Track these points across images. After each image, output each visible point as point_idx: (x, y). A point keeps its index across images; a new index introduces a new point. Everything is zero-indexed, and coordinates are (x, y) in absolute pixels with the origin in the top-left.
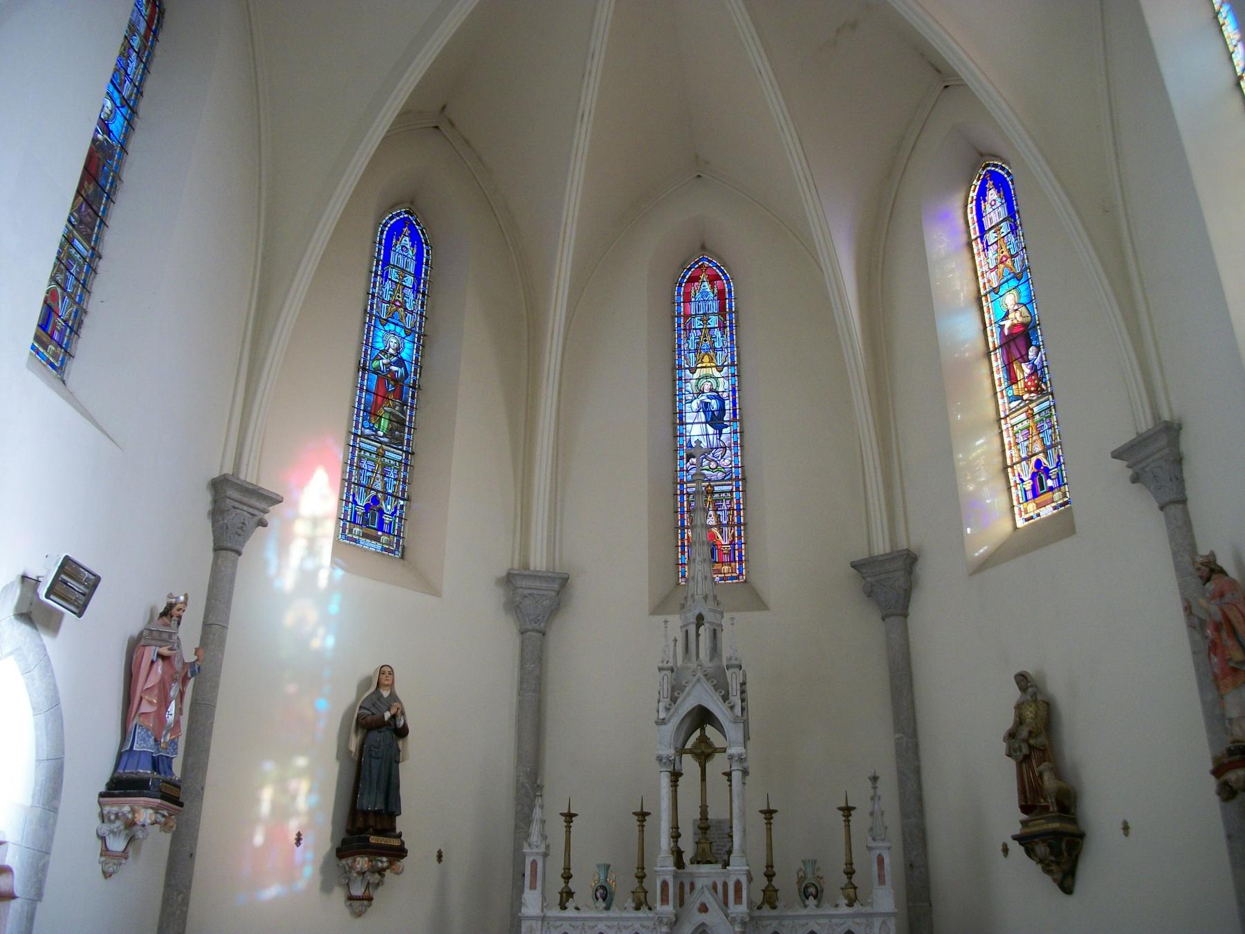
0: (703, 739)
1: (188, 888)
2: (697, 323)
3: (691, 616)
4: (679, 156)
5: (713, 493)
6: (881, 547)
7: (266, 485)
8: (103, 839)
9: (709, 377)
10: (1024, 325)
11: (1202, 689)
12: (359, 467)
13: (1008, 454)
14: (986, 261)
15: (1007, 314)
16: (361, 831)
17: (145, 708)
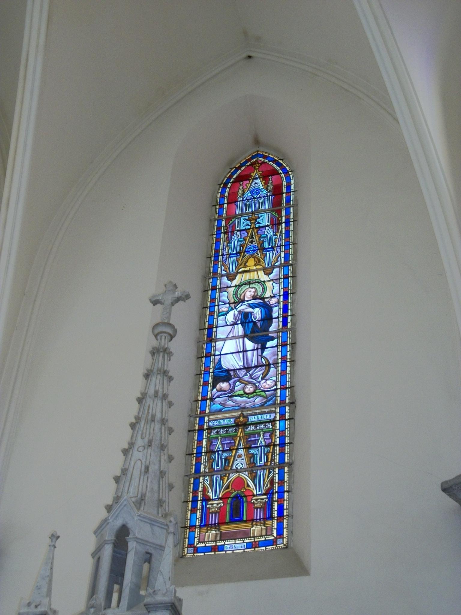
5: (246, 425)
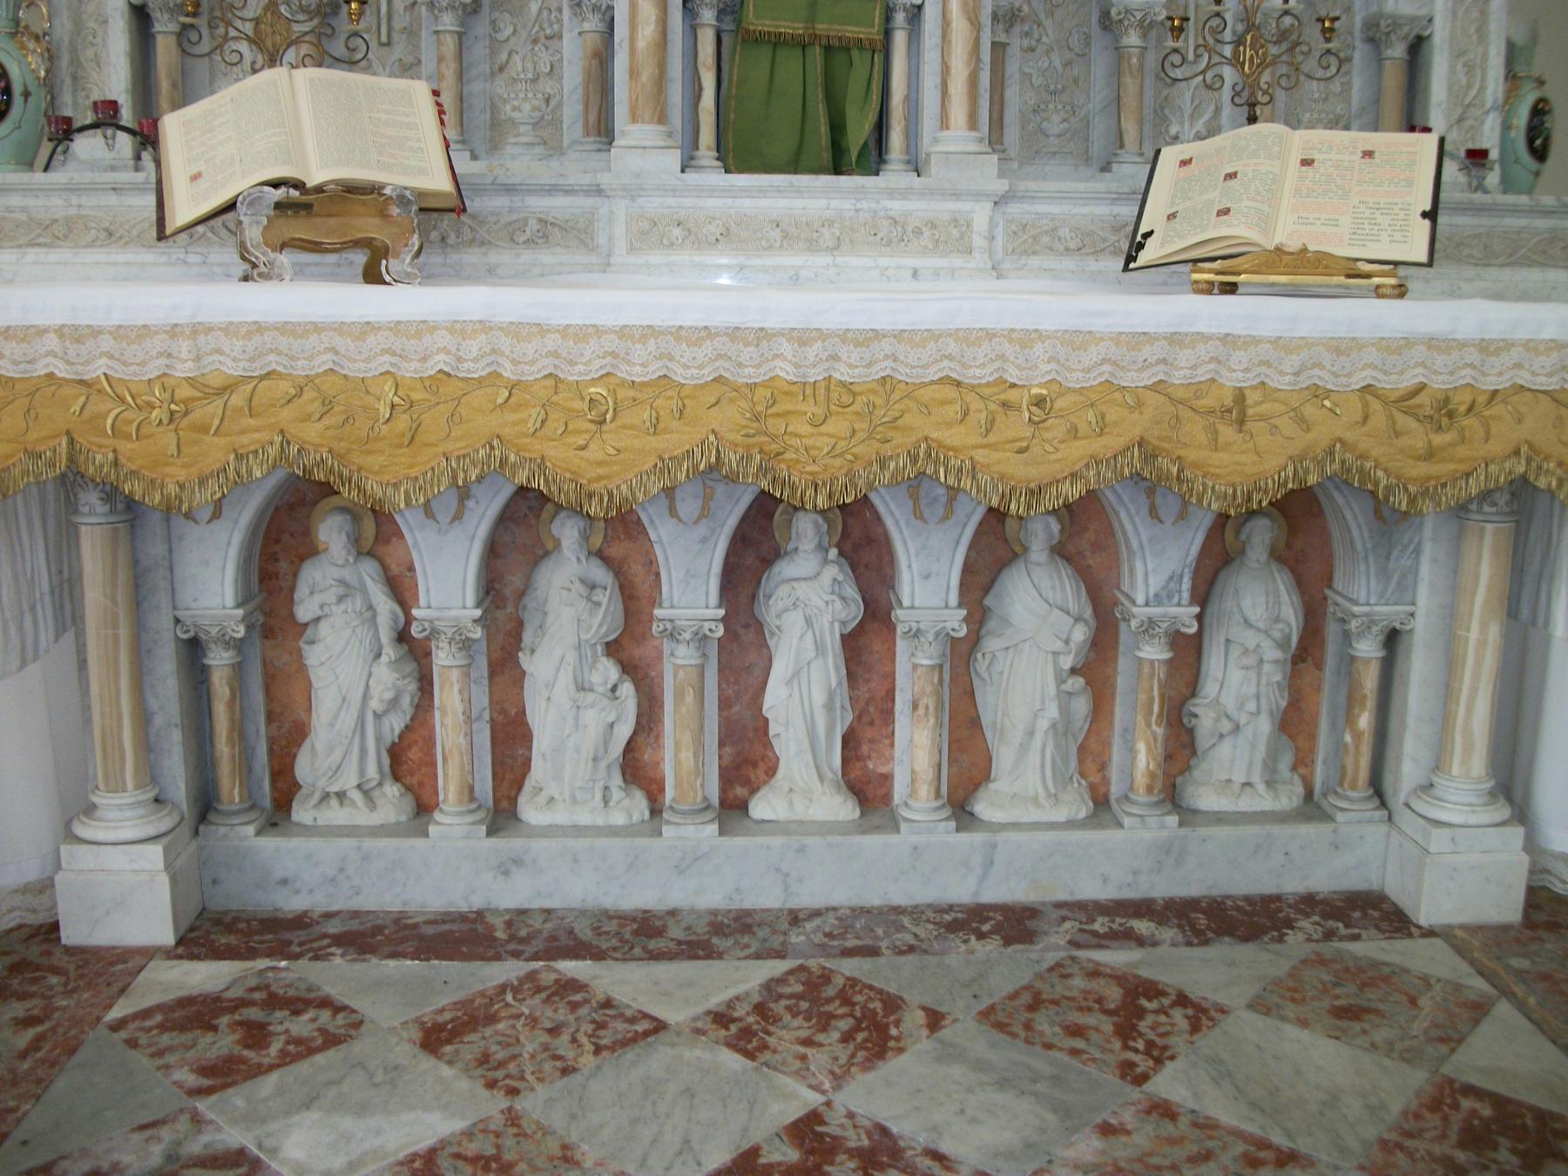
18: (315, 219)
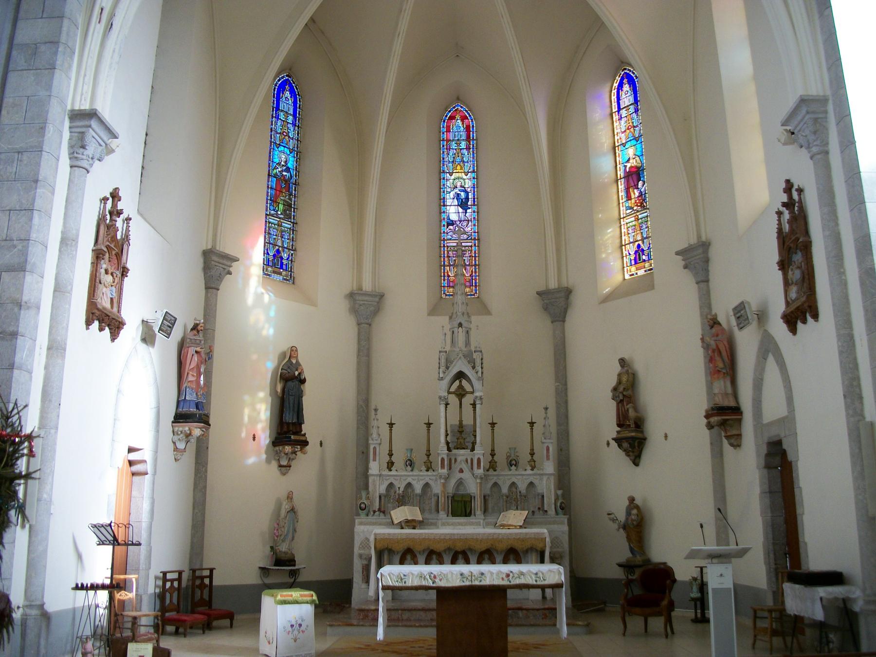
0: (461, 387)
1: (207, 464)
2: (454, 145)
3: (456, 324)
4: (449, 45)
6: (553, 284)
7: (228, 251)
8: (174, 443)
9: (460, 179)
10: (636, 167)
11: (706, 376)
12: (269, 233)
13: (623, 238)
14: (620, 126)
15: (629, 160)
16: (286, 433)
17: (191, 378)
18: (411, 524)
